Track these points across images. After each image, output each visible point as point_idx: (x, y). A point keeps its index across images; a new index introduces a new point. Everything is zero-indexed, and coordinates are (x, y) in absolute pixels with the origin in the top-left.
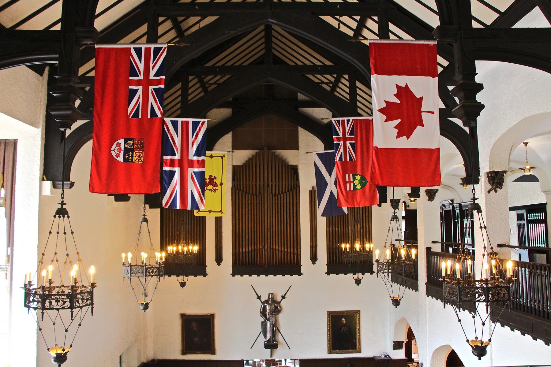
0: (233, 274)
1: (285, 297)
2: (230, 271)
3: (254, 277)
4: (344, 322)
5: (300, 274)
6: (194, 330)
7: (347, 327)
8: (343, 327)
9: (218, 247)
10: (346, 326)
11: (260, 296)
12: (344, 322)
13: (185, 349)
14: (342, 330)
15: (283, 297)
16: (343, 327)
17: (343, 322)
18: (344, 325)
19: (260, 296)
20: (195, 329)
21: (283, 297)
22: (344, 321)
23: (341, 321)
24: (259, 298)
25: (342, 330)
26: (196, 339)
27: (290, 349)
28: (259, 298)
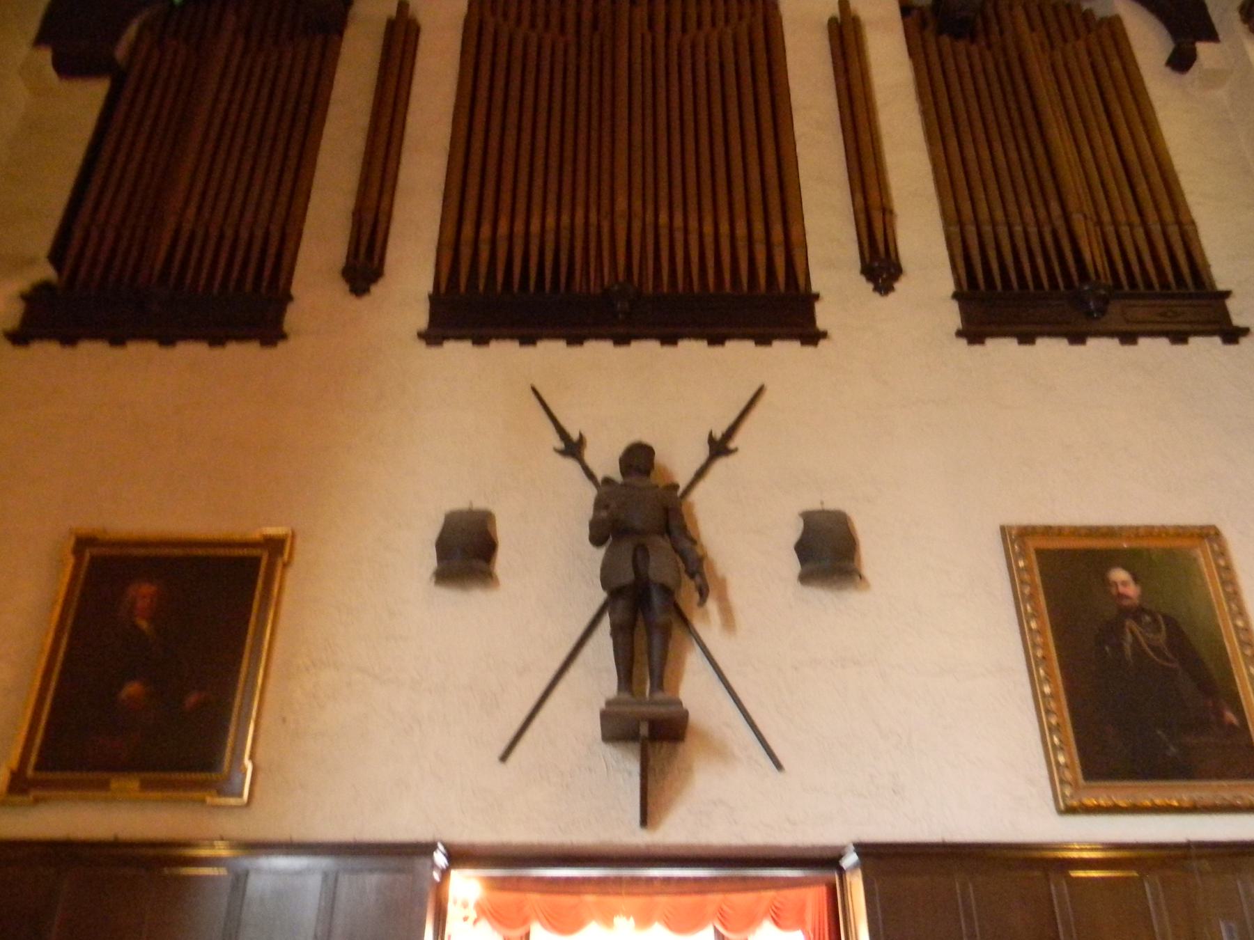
0: (434, 335)
1: (732, 445)
2: (421, 319)
3: (551, 352)
4: (1132, 590)
5: (811, 336)
6: (135, 627)
7: (1155, 620)
8: (1129, 623)
9: (369, 217)
10: (1148, 618)
11: (581, 436)
12: (1132, 590)
13: (33, 759)
14: (1129, 637)
15: (719, 447)
16: (1129, 623)
17: (1122, 589)
18: (1137, 613)
19: (581, 436)
20: (143, 624)
21: (719, 447)
22: (1124, 583)
23: (1106, 583)
24: (573, 448)
25: (1129, 637)
26: (132, 689)
27: (779, 766)
28: (573, 448)
